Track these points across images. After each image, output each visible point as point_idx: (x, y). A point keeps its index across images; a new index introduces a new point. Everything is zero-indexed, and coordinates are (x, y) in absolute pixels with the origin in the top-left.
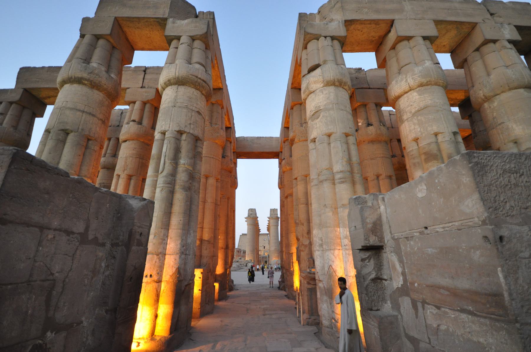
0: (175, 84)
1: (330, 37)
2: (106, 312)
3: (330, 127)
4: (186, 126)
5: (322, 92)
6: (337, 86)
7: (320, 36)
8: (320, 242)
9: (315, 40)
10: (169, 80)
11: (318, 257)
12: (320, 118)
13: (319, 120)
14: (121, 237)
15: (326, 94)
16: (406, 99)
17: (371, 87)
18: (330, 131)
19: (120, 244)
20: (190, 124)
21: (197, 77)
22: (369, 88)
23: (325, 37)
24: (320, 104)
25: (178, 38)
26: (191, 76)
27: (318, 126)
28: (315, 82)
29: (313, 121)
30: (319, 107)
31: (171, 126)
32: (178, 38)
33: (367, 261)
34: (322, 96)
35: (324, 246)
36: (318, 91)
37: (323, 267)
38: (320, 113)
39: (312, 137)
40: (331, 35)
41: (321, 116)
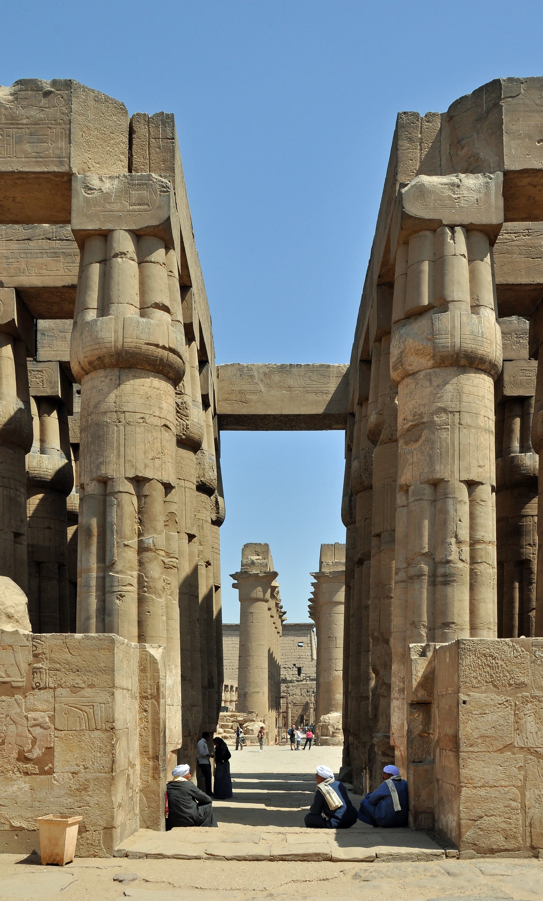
4: (146, 466)
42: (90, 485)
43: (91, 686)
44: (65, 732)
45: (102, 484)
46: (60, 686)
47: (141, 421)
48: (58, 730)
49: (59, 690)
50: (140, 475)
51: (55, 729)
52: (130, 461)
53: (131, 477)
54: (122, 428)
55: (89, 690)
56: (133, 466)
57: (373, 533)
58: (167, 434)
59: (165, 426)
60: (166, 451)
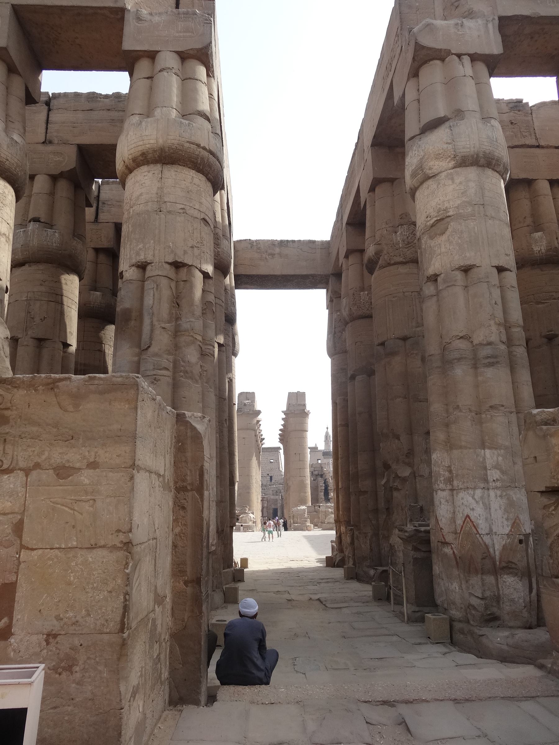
0: (155, 161)
1: (469, 55)
2: (186, 583)
3: (468, 255)
4: (185, 252)
5: (452, 179)
6: (483, 166)
7: (449, 53)
8: (447, 474)
9: (438, 62)
10: (143, 154)
11: (443, 501)
12: (448, 233)
13: (444, 237)
14: (188, 478)
15: (461, 183)
17: (542, 143)
18: (469, 263)
19: (189, 488)
20: (192, 247)
21: (198, 145)
22: (538, 147)
23: (459, 56)
24: (446, 205)
25: (152, 55)
26: (187, 145)
27: (443, 250)
28: (438, 157)
29: (432, 238)
30: (446, 210)
31: (157, 252)
32: (152, 55)
33: (553, 508)
34: (451, 187)
35: (455, 483)
36: (443, 174)
37: (453, 520)
38: (448, 223)
39: (431, 271)
40: (472, 52)
41: (450, 230)
42: (128, 271)
43: (93, 465)
44: (40, 552)
45: (141, 270)
46: (37, 466)
47: (181, 211)
48: (28, 548)
49: (34, 474)
50: (179, 261)
51: (23, 547)
53: (170, 261)
54: (163, 216)
55: (91, 471)
56: (172, 251)
57: (376, 343)
58: (206, 228)
59: (204, 219)
60: (205, 243)
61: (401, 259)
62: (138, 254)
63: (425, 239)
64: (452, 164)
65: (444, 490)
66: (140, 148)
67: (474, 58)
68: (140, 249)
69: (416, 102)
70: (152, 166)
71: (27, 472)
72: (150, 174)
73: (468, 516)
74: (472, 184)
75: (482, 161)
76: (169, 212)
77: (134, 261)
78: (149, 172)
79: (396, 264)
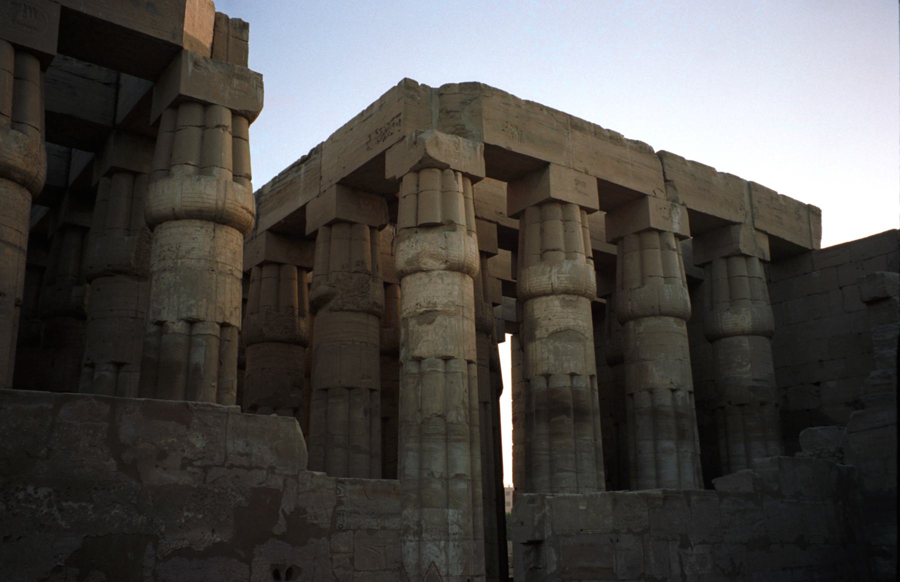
4: (231, 314)
7: (447, 167)
8: (416, 528)
9: (438, 171)
12: (435, 324)
13: (430, 327)
16: (544, 305)
18: (450, 354)
26: (240, 209)
28: (432, 256)
29: (420, 324)
30: (435, 304)
35: (424, 535)
36: (435, 273)
37: (419, 565)
39: (417, 353)
52: (220, 308)
61: (355, 308)
62: (189, 309)
63: (412, 323)
64: (443, 266)
65: (411, 541)
66: (200, 205)
67: (465, 175)
68: (192, 305)
69: (414, 197)
70: (204, 222)
71: (354, 531)
72: (204, 231)
73: (433, 562)
74: (456, 288)
75: (465, 269)
76: (221, 273)
77: (184, 315)
78: (202, 228)
79: (346, 311)
